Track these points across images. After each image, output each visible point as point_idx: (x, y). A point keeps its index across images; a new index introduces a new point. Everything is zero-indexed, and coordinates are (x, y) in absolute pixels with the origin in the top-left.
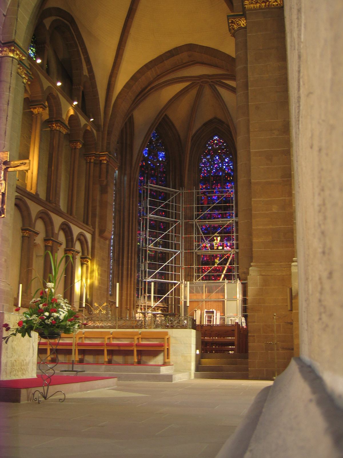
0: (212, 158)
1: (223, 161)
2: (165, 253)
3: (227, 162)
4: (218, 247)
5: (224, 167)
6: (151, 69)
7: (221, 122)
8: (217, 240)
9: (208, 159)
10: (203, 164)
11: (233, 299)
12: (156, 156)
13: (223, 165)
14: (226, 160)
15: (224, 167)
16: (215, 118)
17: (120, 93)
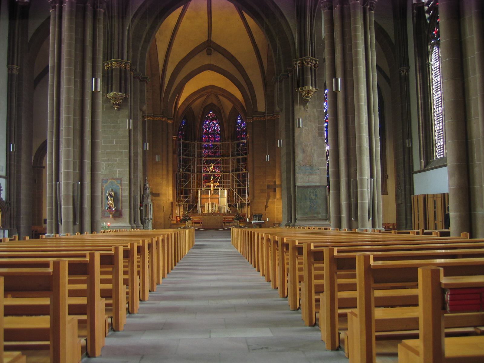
0: (209, 123)
1: (215, 125)
2: (187, 174)
3: (217, 126)
4: (212, 170)
5: (216, 129)
6: (194, 96)
7: (214, 105)
8: (212, 167)
9: (207, 124)
10: (205, 126)
11: (223, 197)
12: (182, 123)
13: (215, 128)
14: (216, 125)
15: (216, 129)
16: (212, 103)
17: (180, 106)
